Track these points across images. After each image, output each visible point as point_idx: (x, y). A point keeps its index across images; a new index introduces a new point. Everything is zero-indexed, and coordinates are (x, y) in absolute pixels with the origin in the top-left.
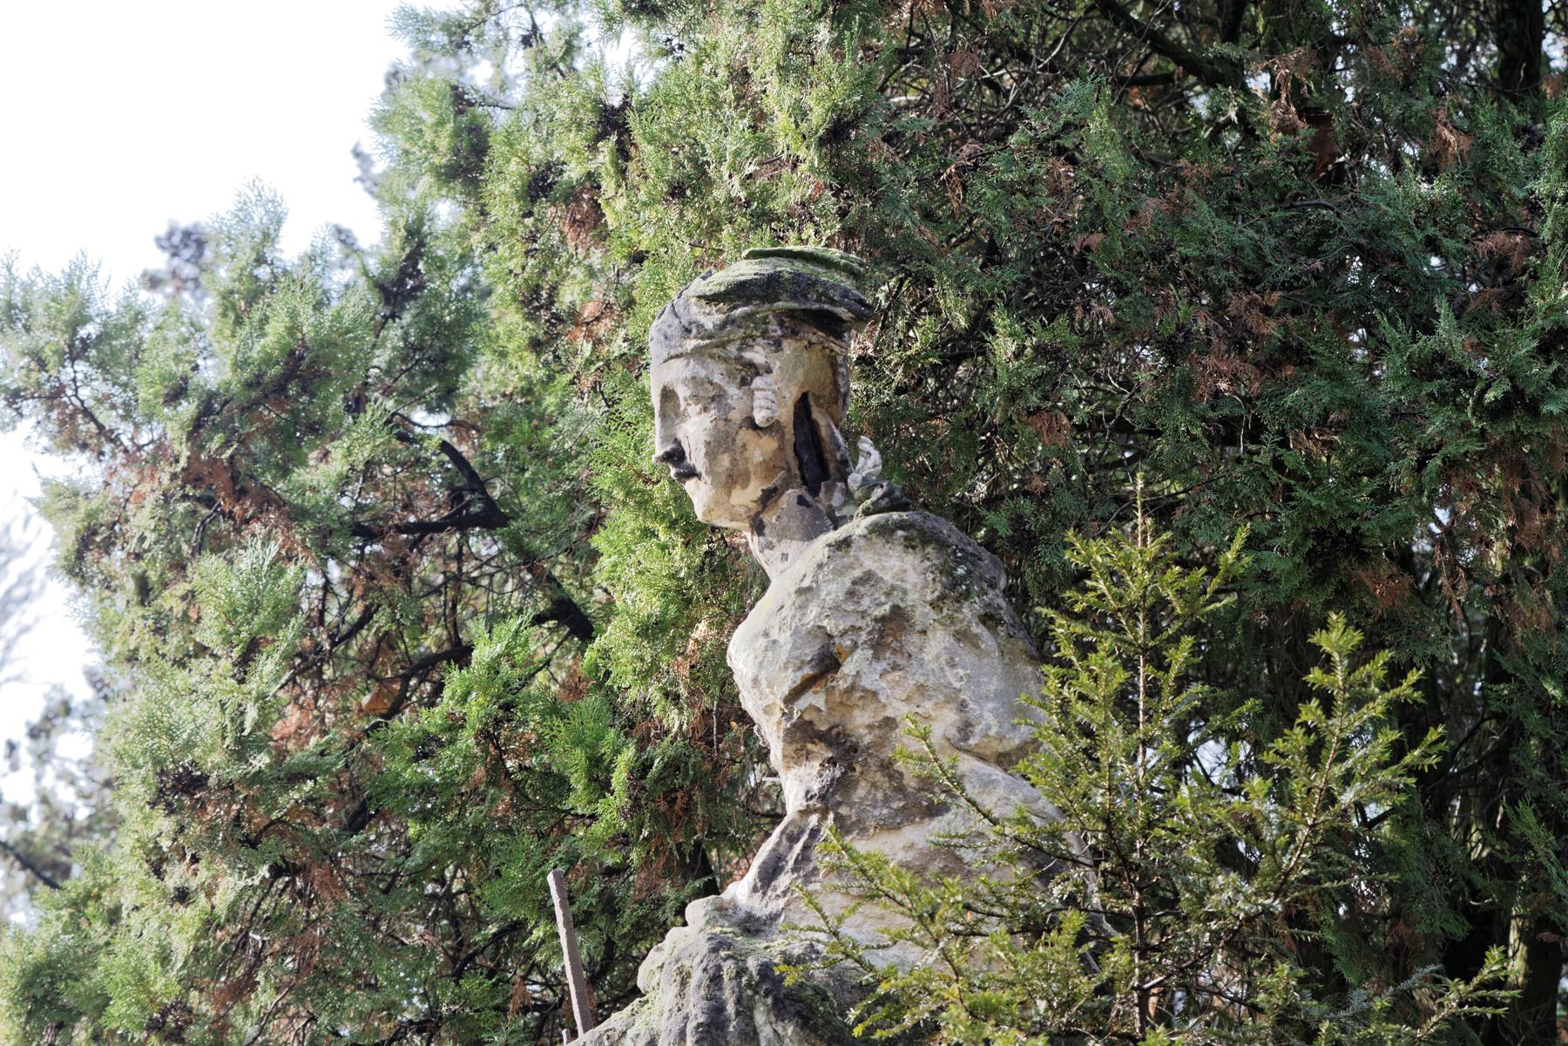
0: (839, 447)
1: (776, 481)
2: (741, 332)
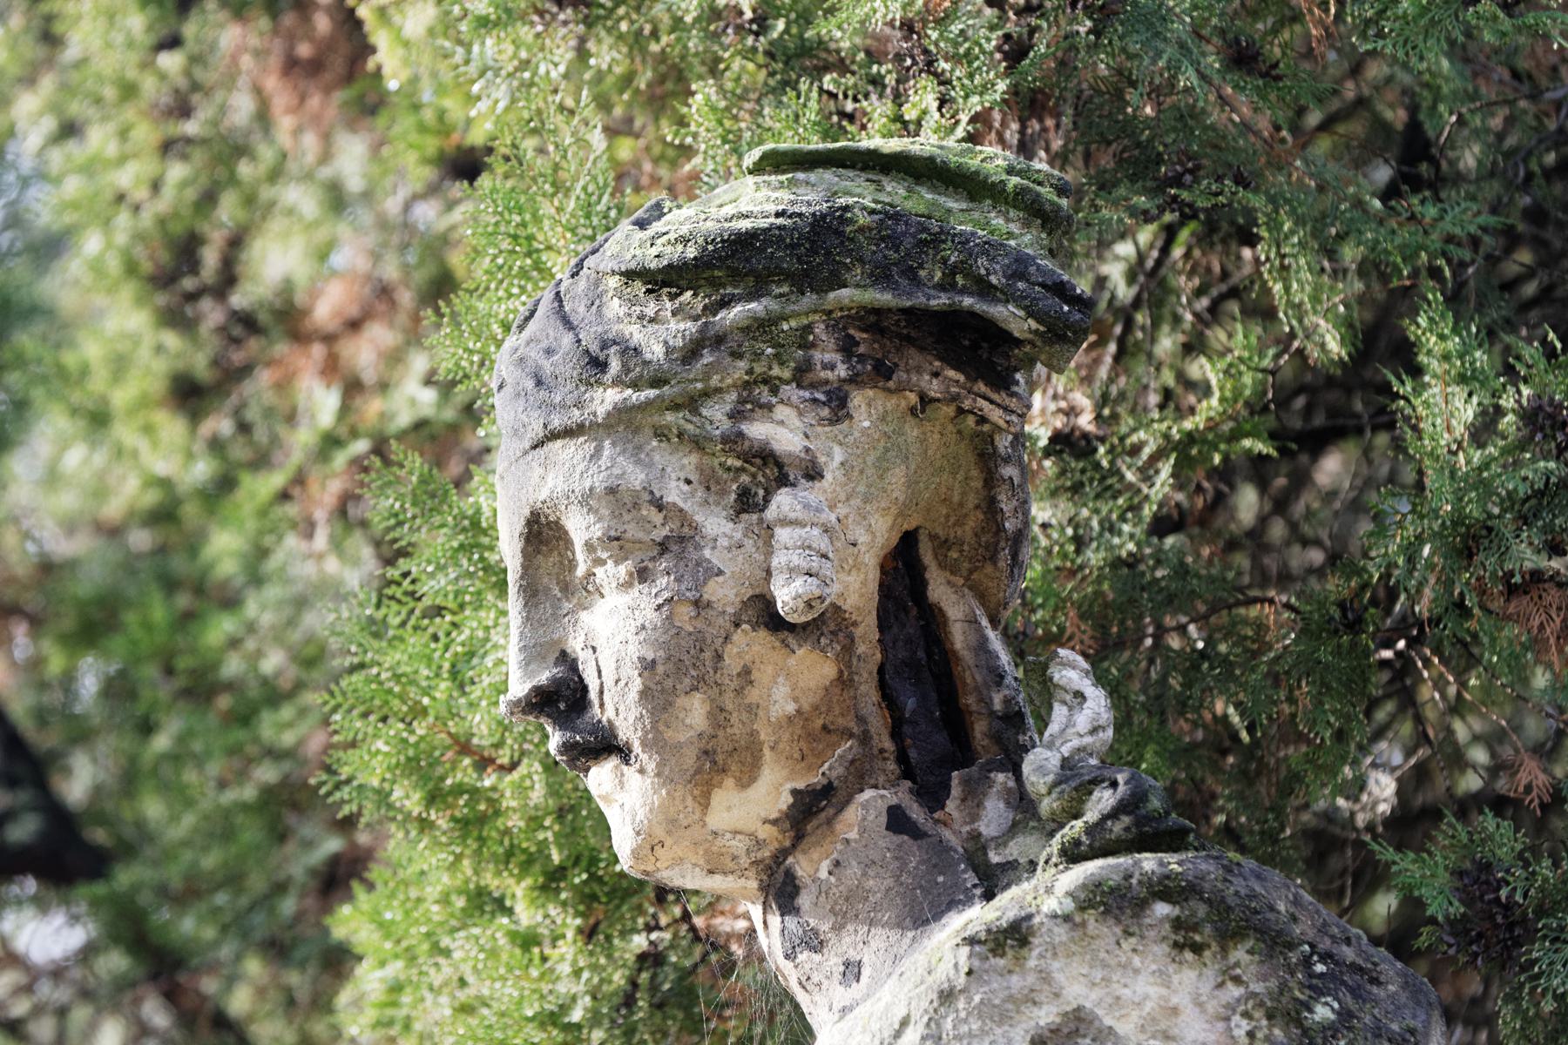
0: (999, 677)
1: (831, 767)
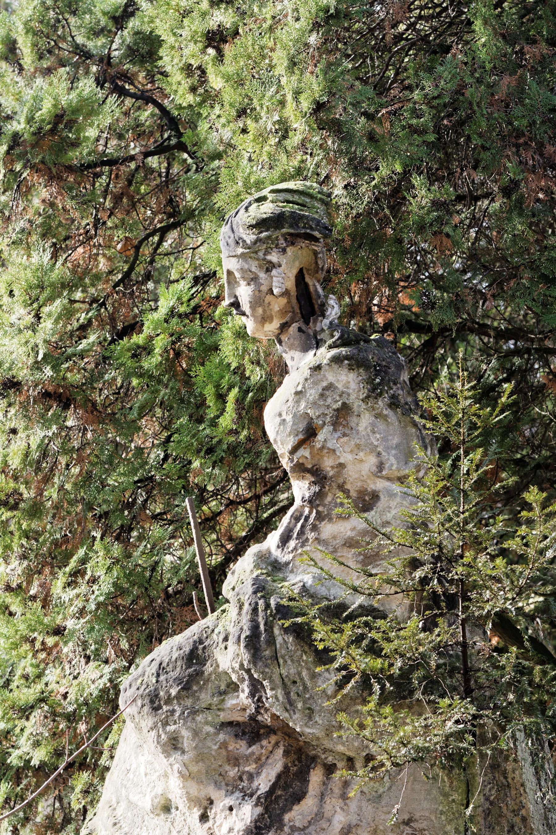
0: (319, 297)
1: (287, 319)
2: (265, 246)
